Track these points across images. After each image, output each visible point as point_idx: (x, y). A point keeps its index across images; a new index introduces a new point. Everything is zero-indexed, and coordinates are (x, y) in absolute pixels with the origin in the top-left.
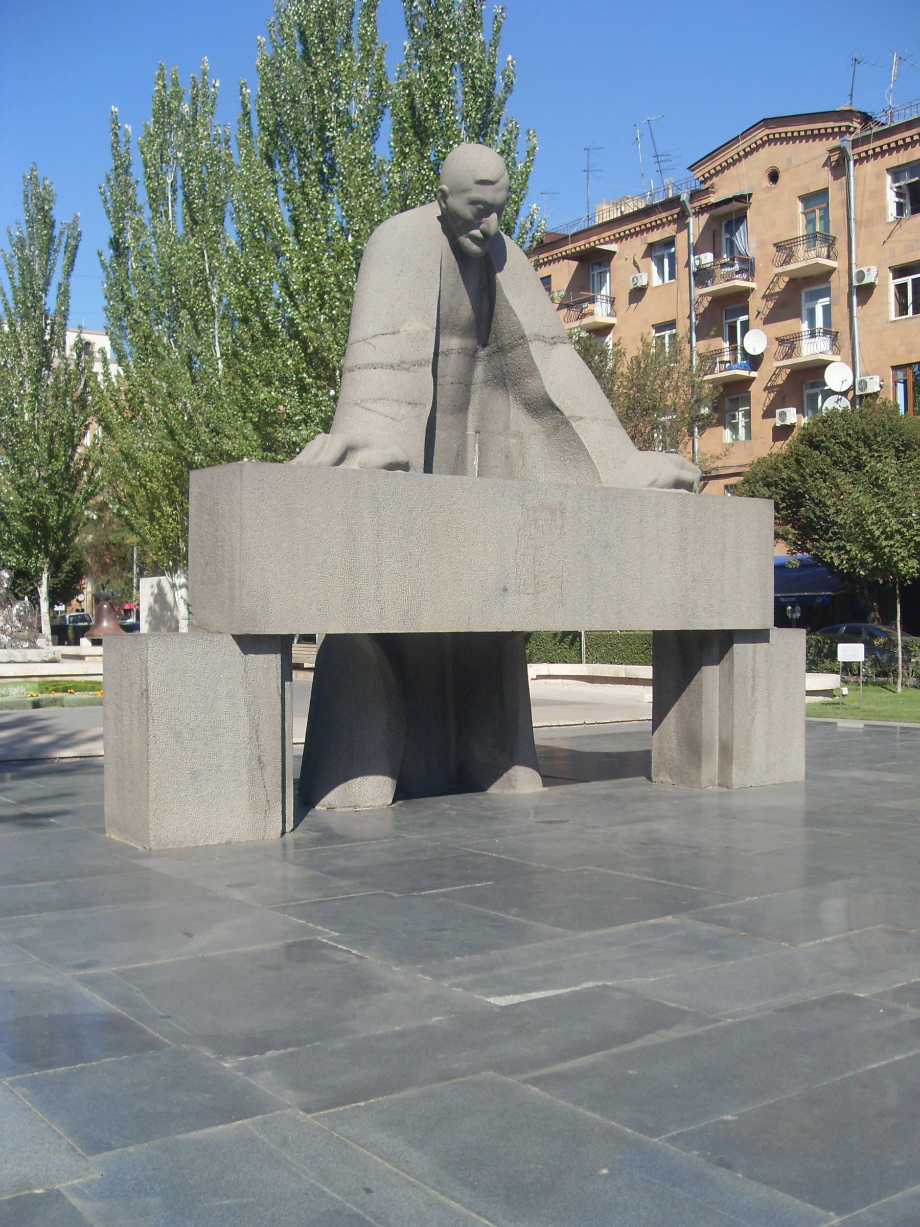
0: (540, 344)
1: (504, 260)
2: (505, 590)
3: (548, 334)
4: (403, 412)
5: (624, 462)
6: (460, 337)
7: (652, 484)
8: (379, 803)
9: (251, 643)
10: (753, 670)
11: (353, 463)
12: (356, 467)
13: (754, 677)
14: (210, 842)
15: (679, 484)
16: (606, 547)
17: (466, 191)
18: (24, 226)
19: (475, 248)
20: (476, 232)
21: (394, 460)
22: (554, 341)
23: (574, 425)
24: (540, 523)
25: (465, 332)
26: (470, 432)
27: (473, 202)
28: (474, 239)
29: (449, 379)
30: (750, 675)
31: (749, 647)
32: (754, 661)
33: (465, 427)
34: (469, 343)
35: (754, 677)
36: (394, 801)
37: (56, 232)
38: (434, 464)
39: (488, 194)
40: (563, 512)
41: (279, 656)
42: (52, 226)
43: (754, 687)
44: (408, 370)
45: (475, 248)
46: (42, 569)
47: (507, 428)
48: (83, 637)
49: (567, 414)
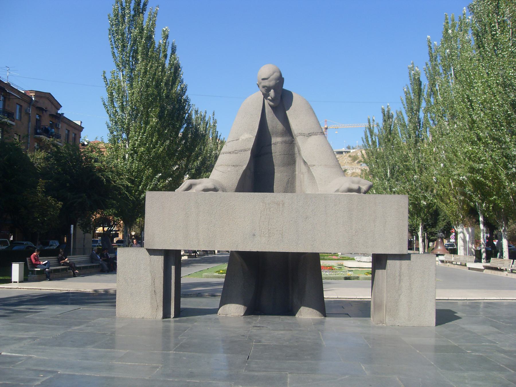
1: (291, 105)
2: (254, 235)
4: (229, 169)
6: (282, 137)
7: (337, 191)
8: (237, 314)
9: (152, 252)
10: (400, 272)
11: (193, 190)
13: (400, 276)
14: (136, 317)
15: (350, 190)
16: (306, 218)
18: (409, 86)
20: (269, 98)
21: (206, 188)
22: (310, 135)
23: (311, 168)
24: (272, 209)
25: (283, 134)
27: (264, 87)
29: (278, 153)
30: (397, 275)
31: (398, 262)
32: (401, 268)
33: (294, 171)
34: (287, 139)
35: (400, 276)
36: (245, 315)
37: (422, 87)
38: (274, 186)
39: (266, 83)
40: (283, 205)
42: (420, 85)
43: (400, 281)
44: (237, 153)
46: (419, 225)
49: (309, 164)
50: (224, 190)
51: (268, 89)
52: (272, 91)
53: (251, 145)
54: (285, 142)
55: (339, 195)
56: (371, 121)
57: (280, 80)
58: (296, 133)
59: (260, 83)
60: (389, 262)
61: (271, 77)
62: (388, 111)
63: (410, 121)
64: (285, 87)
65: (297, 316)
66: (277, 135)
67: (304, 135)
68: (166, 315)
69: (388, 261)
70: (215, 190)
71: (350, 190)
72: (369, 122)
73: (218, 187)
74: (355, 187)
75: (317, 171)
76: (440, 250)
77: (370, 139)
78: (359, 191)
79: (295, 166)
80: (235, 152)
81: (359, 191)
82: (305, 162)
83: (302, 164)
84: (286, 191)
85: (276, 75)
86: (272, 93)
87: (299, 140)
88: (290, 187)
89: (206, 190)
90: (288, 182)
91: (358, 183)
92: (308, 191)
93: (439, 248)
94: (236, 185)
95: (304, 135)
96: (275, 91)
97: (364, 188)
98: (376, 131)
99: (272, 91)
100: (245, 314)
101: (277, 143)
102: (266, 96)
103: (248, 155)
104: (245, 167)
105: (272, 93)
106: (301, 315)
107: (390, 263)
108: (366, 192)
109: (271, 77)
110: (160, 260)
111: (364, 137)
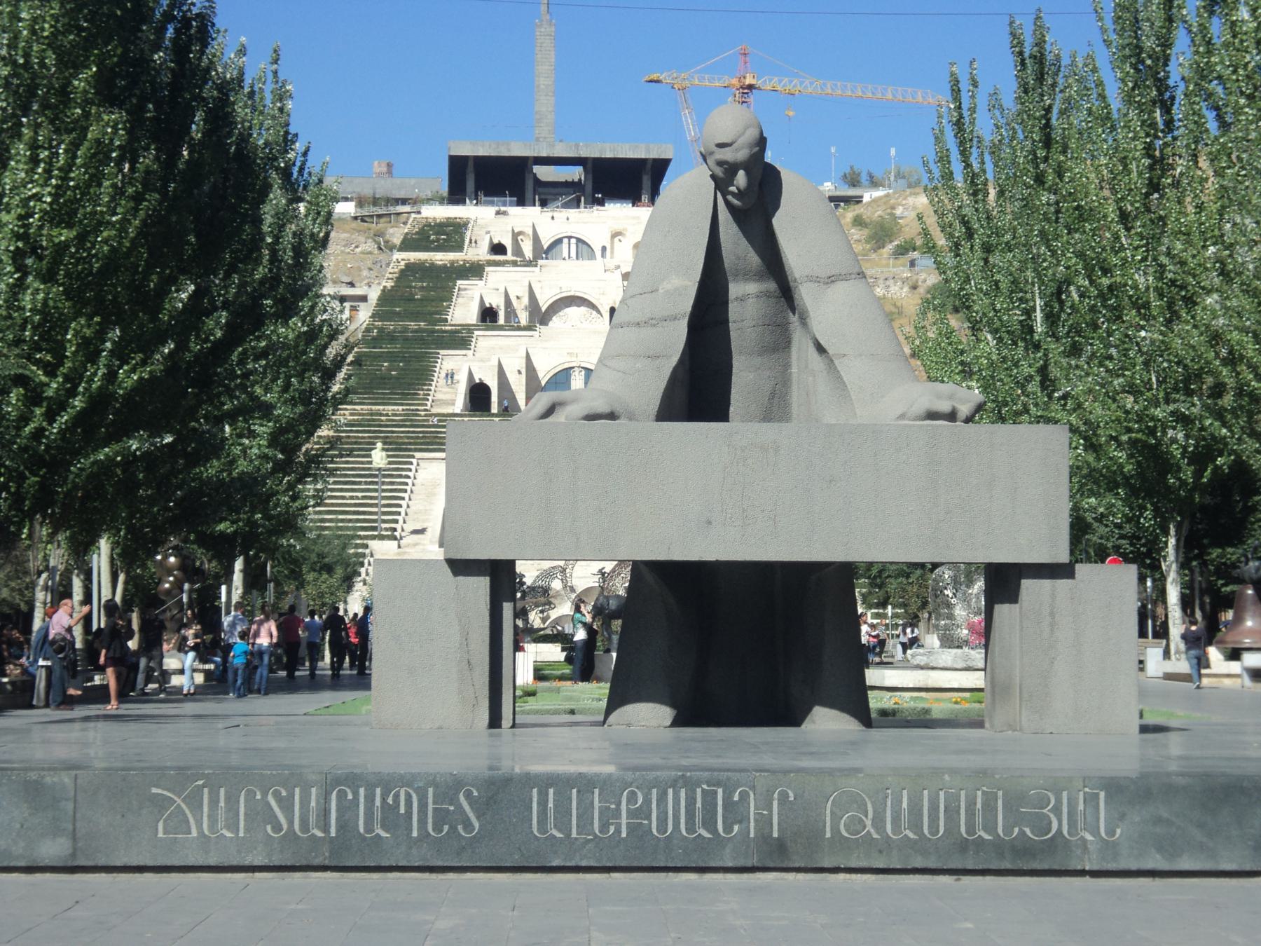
0: (812, 285)
2: (709, 522)
3: (824, 273)
4: (639, 365)
5: (883, 397)
6: (758, 280)
7: (902, 416)
8: (654, 723)
9: (460, 567)
11: (559, 417)
12: (562, 419)
13: (1052, 614)
15: (932, 415)
17: (712, 153)
19: (735, 202)
20: (733, 189)
21: (592, 412)
22: (831, 280)
23: (836, 362)
24: (750, 461)
25: (759, 277)
26: (794, 370)
27: (720, 163)
28: (733, 194)
29: (748, 323)
31: (1046, 584)
33: (787, 366)
35: (1052, 614)
40: (776, 450)
41: (488, 579)
45: (735, 202)
47: (806, 367)
48: (1210, 644)
49: (831, 352)
50: (631, 417)
51: (730, 169)
52: (741, 173)
53: (687, 304)
54: (767, 294)
55: (906, 425)
56: (965, 85)
57: (762, 142)
58: (797, 276)
59: (712, 153)
60: (1026, 584)
61: (740, 141)
62: (1040, 43)
63: (1129, 99)
64: (769, 157)
65: (803, 726)
66: (746, 276)
67: (816, 280)
68: (495, 721)
69: (1023, 581)
70: (612, 416)
71: (932, 415)
72: (956, 92)
73: (618, 409)
74: (945, 407)
75: (851, 370)
76: (1251, 632)
77: (957, 167)
78: (952, 416)
79: (789, 352)
80: (649, 323)
81: (952, 416)
82: (820, 349)
83: (812, 350)
84: (767, 417)
85: (752, 134)
86: (741, 178)
87: (805, 294)
88: (775, 408)
89: (591, 417)
90: (773, 395)
91: (951, 397)
92: (829, 419)
93: (1249, 623)
94: (658, 403)
95: (816, 280)
96: (748, 174)
97: (964, 410)
98: (984, 126)
99: (741, 173)
100: (677, 723)
101: (746, 298)
102: (721, 184)
103: (678, 334)
104: (675, 360)
105: (741, 178)
106: (814, 722)
107: (1029, 586)
108: (969, 420)
109: (740, 141)
110: (481, 585)
111: (931, 156)
